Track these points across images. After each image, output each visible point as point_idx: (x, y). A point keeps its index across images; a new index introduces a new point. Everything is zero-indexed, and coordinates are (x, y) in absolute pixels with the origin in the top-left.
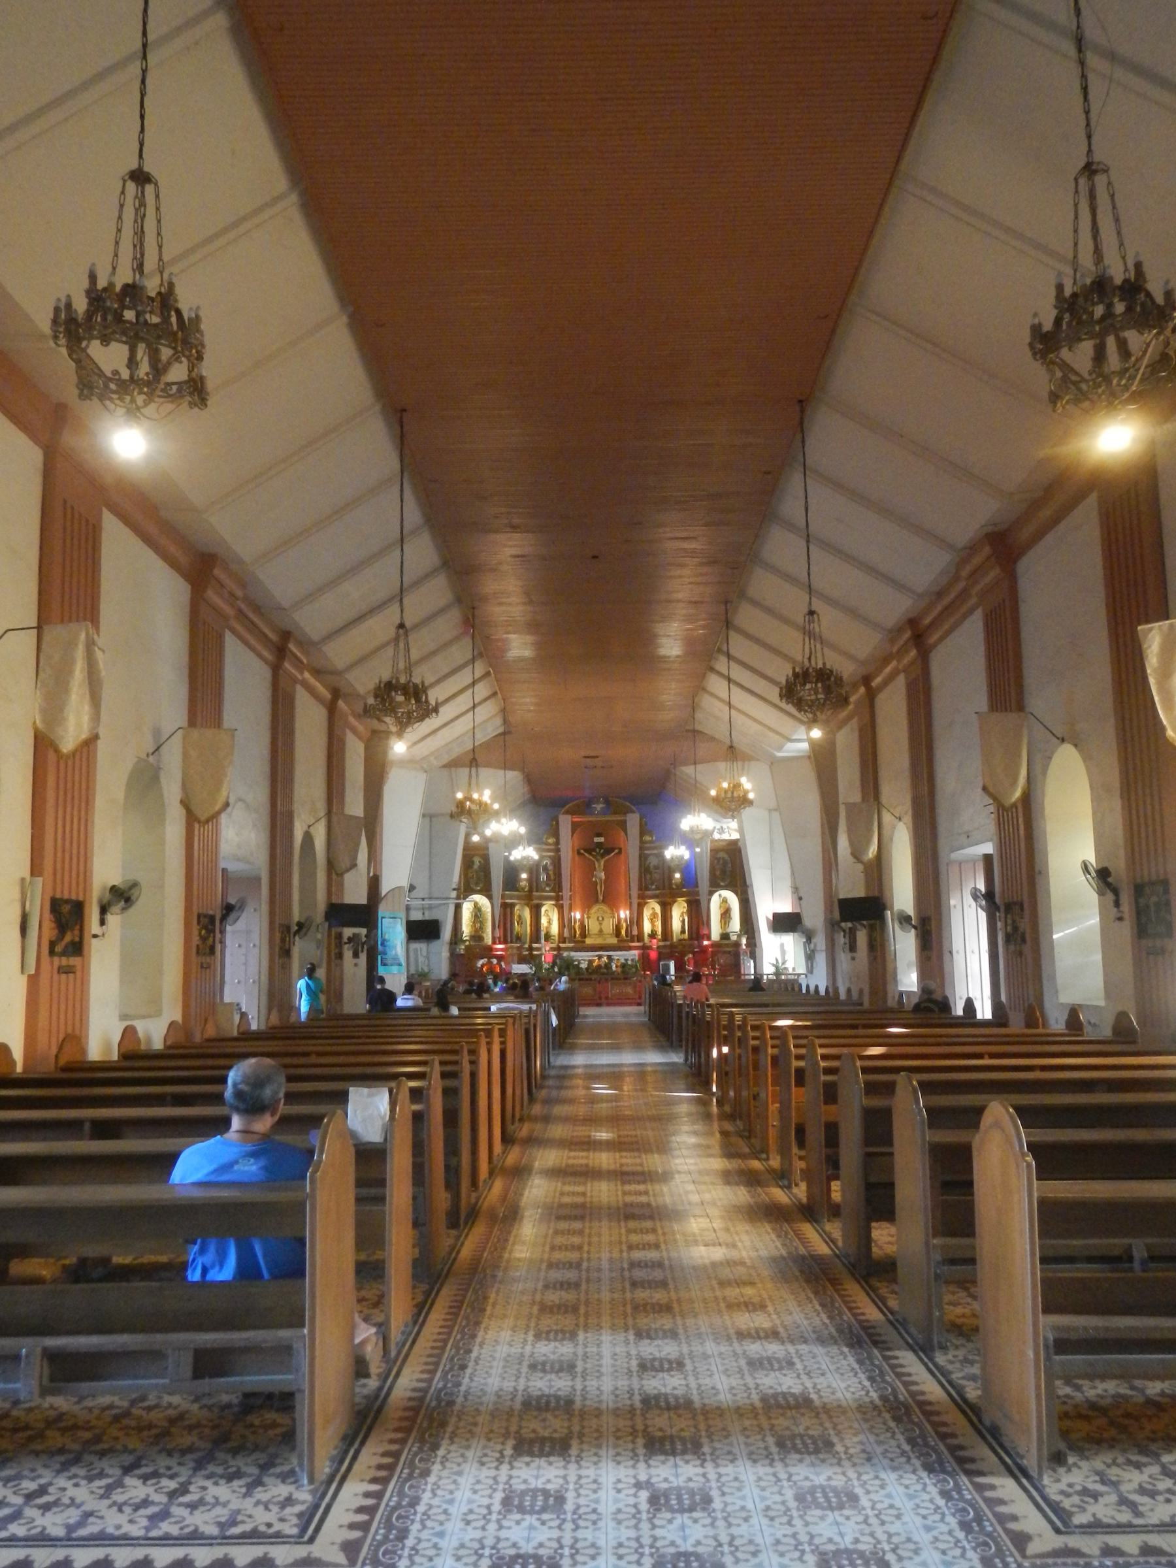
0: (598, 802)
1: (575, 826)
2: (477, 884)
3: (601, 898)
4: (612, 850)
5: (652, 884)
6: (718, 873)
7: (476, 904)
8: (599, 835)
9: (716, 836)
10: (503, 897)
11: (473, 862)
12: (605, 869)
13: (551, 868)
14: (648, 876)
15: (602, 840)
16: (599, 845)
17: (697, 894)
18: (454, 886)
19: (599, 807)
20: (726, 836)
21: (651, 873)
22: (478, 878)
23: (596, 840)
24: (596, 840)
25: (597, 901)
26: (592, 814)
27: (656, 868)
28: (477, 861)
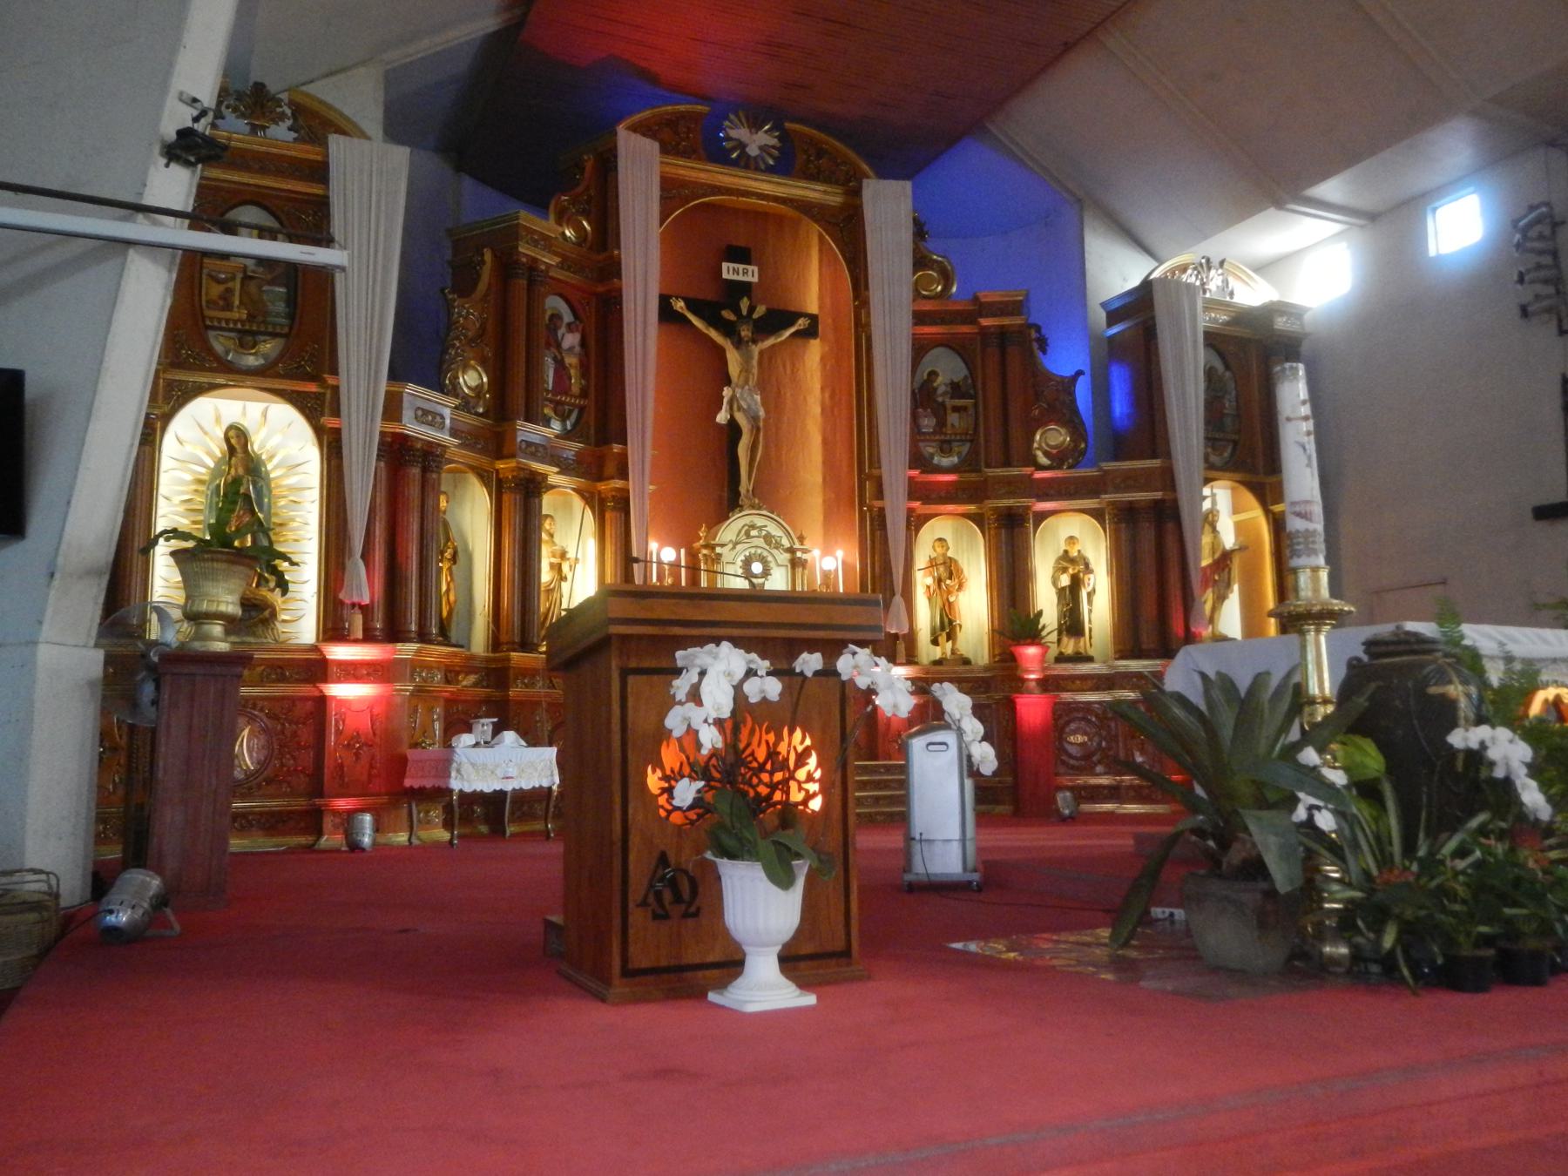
0: (755, 125)
1: (672, 192)
2: (247, 338)
3: (745, 486)
4: (787, 318)
7: (237, 441)
8: (741, 255)
10: (393, 408)
12: (762, 386)
13: (570, 340)
15: (748, 274)
17: (1167, 478)
18: (176, 117)
19: (758, 141)
22: (257, 314)
23: (729, 271)
24: (729, 271)
25: (731, 503)
26: (735, 164)
27: (956, 389)
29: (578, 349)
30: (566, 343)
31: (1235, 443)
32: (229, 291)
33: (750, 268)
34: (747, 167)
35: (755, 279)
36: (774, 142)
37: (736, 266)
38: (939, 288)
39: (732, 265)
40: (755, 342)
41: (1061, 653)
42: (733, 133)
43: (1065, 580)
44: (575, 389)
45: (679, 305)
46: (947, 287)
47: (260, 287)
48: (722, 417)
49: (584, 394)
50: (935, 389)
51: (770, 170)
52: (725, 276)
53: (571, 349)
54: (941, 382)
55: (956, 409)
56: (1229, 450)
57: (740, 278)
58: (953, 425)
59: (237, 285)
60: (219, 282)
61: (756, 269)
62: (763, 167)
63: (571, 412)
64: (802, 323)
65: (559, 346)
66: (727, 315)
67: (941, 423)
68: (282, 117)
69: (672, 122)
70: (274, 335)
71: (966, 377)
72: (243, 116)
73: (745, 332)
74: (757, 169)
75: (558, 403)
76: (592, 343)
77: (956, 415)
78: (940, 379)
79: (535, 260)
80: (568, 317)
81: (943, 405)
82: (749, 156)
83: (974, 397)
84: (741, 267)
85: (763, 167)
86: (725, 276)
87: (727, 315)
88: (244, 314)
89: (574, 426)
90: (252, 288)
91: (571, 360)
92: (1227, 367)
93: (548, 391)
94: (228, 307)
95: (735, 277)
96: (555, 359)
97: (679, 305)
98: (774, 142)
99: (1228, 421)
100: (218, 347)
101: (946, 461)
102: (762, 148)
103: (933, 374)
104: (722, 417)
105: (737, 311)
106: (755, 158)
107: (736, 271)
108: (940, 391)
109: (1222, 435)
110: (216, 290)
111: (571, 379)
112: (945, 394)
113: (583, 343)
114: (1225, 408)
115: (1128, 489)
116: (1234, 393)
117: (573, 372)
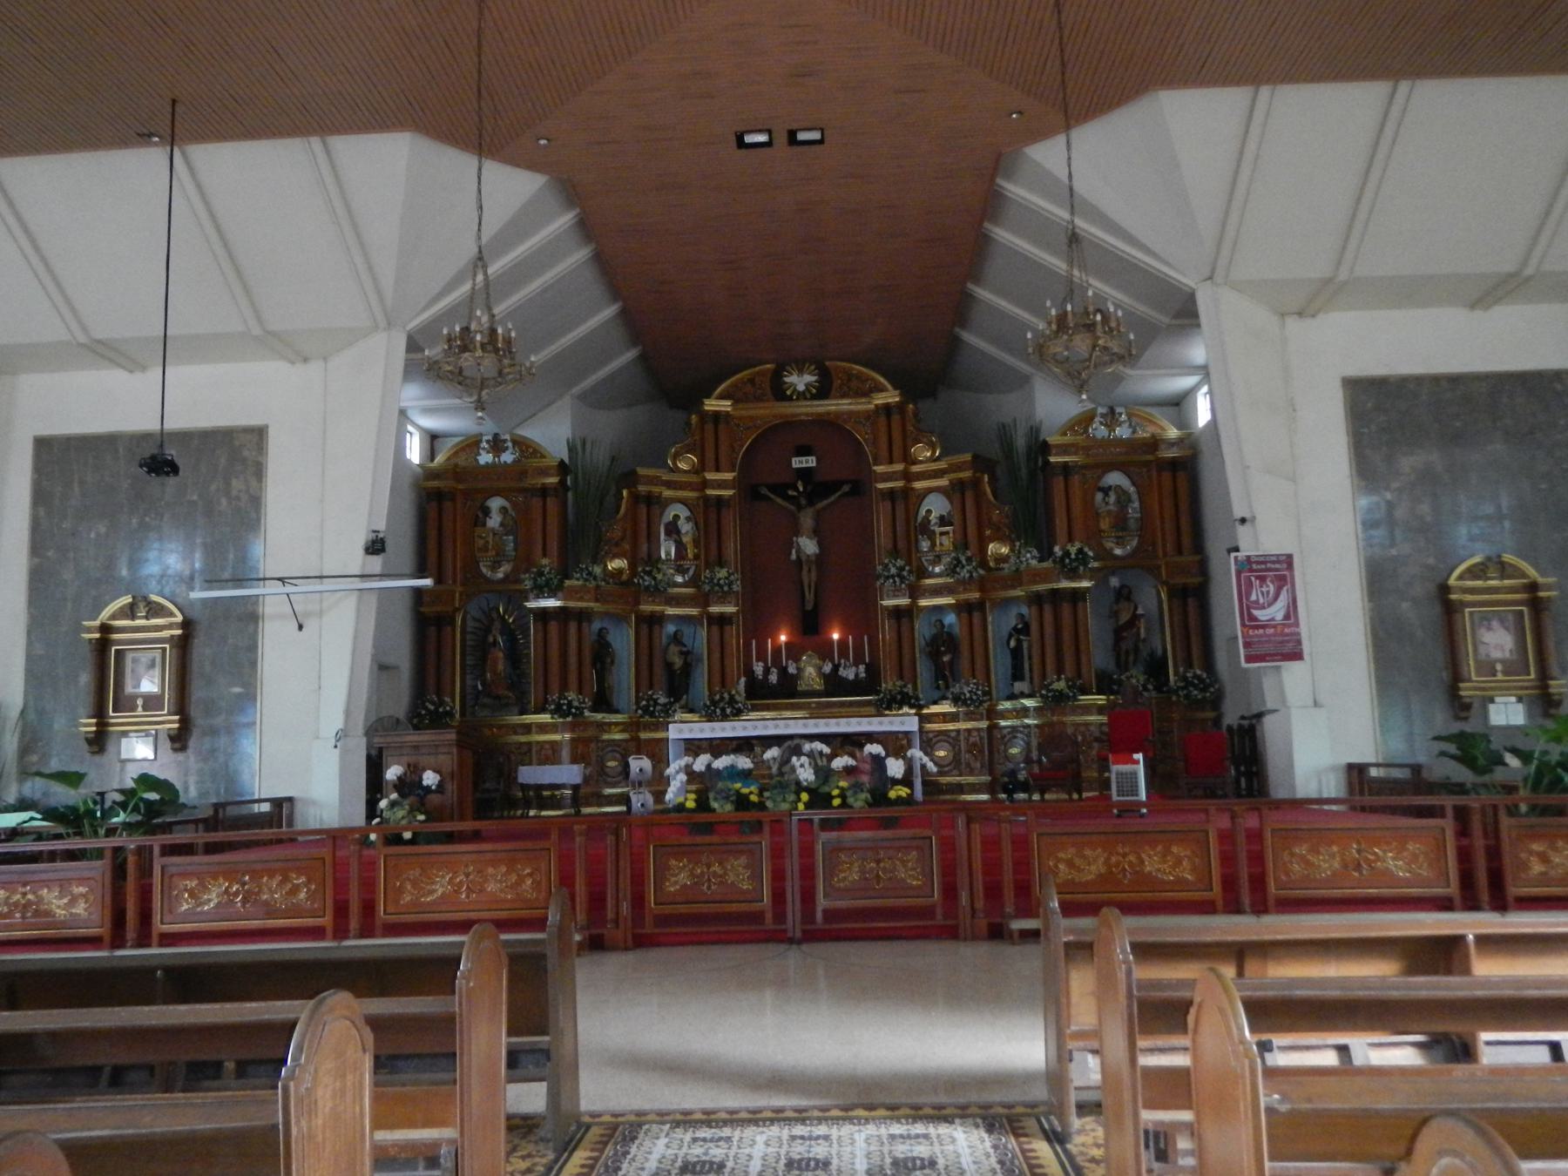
0: (801, 372)
5: (937, 560)
6: (1105, 524)
8: (803, 451)
9: (1099, 430)
11: (487, 512)
13: (686, 527)
14: (925, 545)
15: (810, 462)
16: (805, 473)
19: (800, 381)
20: (1123, 432)
21: (931, 536)
23: (798, 463)
24: (798, 463)
26: (790, 399)
27: (943, 521)
28: (496, 503)
29: (691, 532)
30: (683, 531)
31: (1140, 536)
32: (487, 542)
33: (810, 458)
34: (798, 399)
35: (814, 465)
36: (814, 378)
37: (800, 458)
38: (929, 454)
39: (797, 459)
40: (811, 503)
41: (1013, 693)
42: (786, 379)
43: (1013, 643)
44: (690, 556)
45: (764, 491)
46: (934, 453)
47: (501, 538)
48: (794, 556)
49: (696, 557)
50: (930, 521)
51: (814, 397)
52: (794, 466)
53: (687, 533)
54: (933, 517)
55: (942, 534)
56: (1135, 542)
57: (804, 465)
58: (941, 544)
59: (490, 539)
60: (481, 537)
61: (814, 458)
62: (808, 396)
63: (688, 569)
64: (846, 488)
65: (678, 532)
66: (791, 493)
67: (933, 545)
68: (507, 448)
69: (751, 381)
70: (508, 561)
71: (949, 513)
72: (488, 452)
73: (803, 502)
74: (806, 399)
75: (681, 566)
76: (702, 526)
77: (944, 537)
78: (933, 515)
79: (650, 492)
80: (683, 512)
81: (934, 532)
82: (799, 392)
83: (951, 524)
84: (804, 459)
85: (808, 396)
86: (794, 466)
87: (791, 493)
88: (494, 553)
89: (690, 579)
90: (497, 537)
91: (685, 539)
92: (1134, 484)
93: (670, 560)
94: (487, 550)
95: (801, 466)
96: (676, 541)
97: (764, 491)
98: (814, 378)
99: (1132, 524)
100: (484, 570)
101: (937, 570)
102: (807, 385)
103: (929, 512)
104: (794, 556)
105: (796, 489)
106: (804, 392)
107: (801, 462)
108: (932, 523)
109: (1124, 533)
110: (481, 542)
111: (686, 550)
112: (936, 524)
113: (696, 524)
114: (1128, 513)
115: (1035, 583)
116: (1136, 504)
117: (688, 546)
